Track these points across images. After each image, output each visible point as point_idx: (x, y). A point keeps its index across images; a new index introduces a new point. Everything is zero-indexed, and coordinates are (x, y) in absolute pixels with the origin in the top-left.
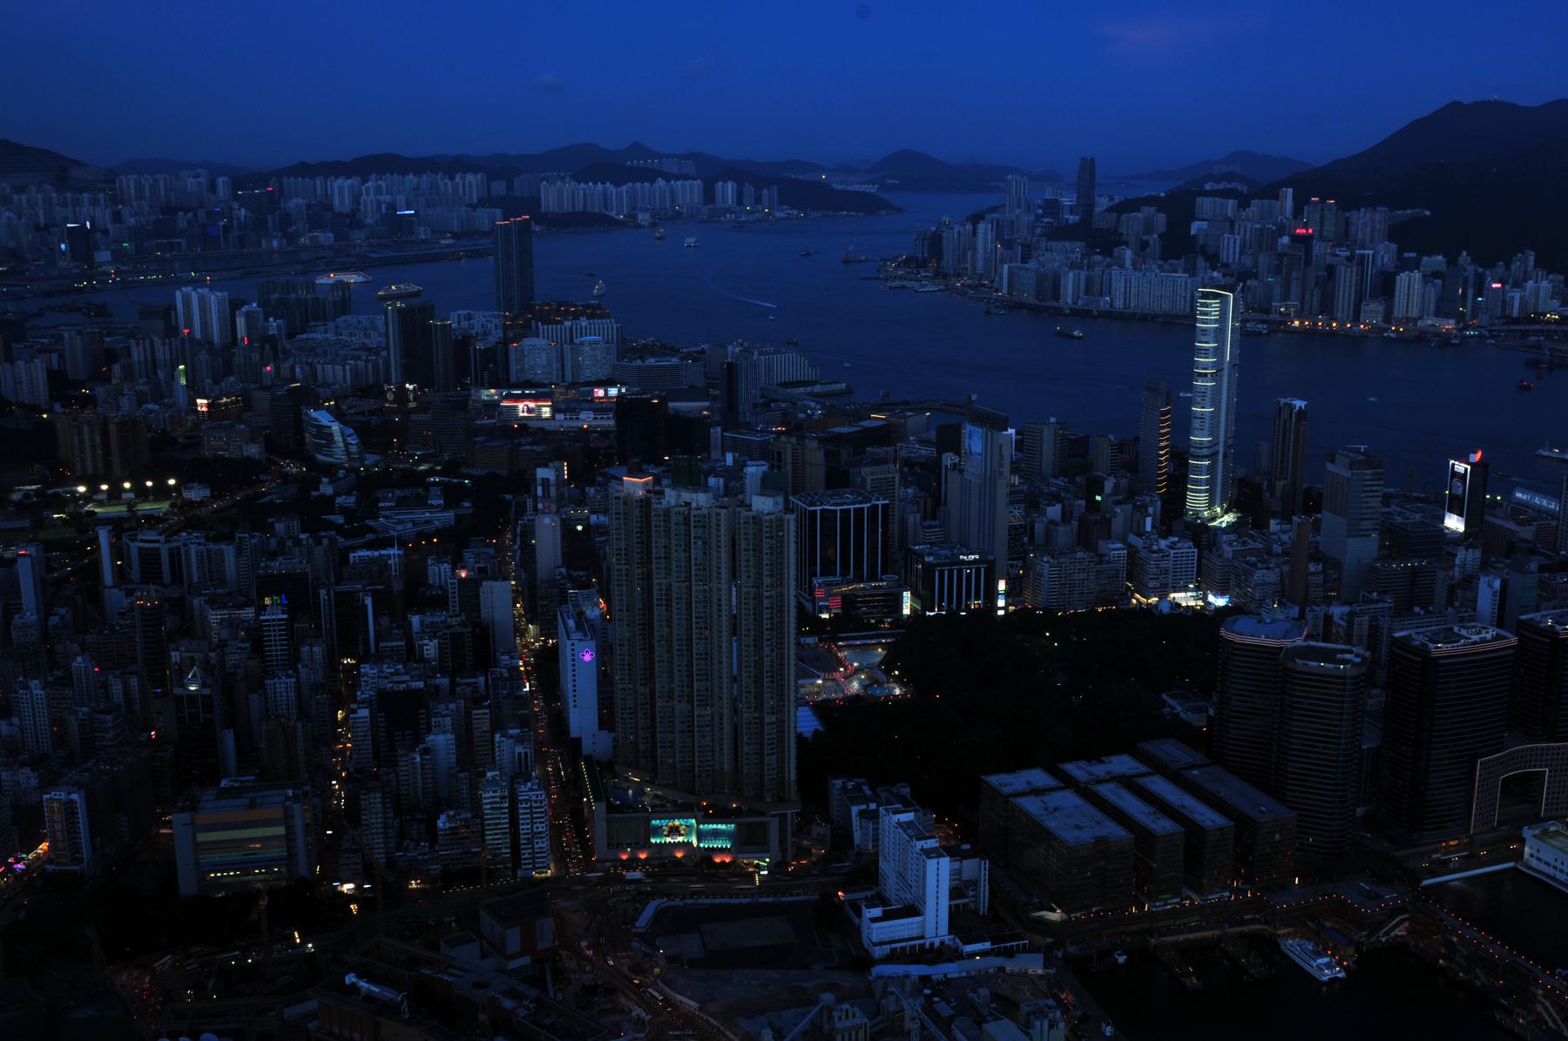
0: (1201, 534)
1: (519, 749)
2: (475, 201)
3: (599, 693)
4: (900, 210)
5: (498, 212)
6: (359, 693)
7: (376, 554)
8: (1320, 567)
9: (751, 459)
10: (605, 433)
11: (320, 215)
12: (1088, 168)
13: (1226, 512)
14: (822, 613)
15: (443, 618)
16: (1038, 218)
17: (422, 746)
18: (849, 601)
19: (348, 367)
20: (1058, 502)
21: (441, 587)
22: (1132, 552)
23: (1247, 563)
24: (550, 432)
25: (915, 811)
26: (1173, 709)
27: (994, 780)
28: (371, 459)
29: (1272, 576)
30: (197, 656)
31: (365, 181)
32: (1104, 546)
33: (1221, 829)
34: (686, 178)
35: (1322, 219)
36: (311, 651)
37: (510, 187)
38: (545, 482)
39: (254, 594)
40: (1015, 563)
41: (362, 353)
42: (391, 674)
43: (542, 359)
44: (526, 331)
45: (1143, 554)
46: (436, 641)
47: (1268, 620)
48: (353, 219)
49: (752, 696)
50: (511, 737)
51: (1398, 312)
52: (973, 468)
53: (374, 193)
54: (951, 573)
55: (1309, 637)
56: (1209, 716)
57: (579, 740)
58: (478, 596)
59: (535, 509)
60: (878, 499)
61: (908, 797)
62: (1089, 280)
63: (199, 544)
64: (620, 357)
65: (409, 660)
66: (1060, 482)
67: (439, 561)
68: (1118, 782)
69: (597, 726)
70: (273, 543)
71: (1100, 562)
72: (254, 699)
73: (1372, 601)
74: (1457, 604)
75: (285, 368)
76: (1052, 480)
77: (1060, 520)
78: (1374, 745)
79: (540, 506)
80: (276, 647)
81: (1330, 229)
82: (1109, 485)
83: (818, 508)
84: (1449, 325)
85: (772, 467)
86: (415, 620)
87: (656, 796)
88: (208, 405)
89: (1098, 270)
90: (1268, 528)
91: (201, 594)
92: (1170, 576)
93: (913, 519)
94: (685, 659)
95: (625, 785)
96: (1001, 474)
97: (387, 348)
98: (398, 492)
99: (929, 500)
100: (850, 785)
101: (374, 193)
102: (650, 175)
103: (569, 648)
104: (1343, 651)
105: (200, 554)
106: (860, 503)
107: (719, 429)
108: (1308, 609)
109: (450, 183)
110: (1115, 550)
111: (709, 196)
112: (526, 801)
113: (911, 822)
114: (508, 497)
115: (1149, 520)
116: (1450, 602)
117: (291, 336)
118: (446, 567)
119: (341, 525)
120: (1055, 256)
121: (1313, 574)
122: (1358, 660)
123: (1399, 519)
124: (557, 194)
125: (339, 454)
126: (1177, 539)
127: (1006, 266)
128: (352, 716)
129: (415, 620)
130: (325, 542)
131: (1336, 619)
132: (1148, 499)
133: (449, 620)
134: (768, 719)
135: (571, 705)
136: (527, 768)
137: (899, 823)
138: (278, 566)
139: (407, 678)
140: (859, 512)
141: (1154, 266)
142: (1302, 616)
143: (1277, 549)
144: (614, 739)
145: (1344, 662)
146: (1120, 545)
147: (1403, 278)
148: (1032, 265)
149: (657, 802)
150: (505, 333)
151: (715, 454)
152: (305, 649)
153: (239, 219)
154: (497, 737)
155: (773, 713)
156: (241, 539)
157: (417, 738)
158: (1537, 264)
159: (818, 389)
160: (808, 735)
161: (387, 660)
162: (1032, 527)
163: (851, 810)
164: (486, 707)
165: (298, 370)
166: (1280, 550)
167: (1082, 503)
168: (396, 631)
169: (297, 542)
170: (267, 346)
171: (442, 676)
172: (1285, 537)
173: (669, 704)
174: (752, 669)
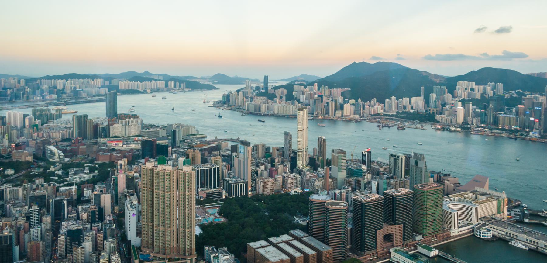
0: (300, 172)
1: (112, 245)
2: (100, 86)
3: (137, 226)
4: (218, 89)
5: (107, 90)
6: (61, 231)
7: (68, 188)
8: (332, 180)
9: (180, 156)
10: (138, 150)
11: (53, 90)
12: (266, 78)
13: (307, 166)
14: (200, 198)
15: (89, 206)
16: (254, 91)
17: (81, 246)
18: (208, 195)
19: (60, 133)
20: (264, 165)
21: (88, 197)
22: (284, 177)
23: (314, 180)
24: (122, 150)
25: (229, 255)
26: (297, 220)
27: (251, 244)
28: (67, 160)
29: (320, 183)
30: (8, 223)
31: (67, 81)
32: (276, 176)
33: (313, 254)
34: (160, 80)
35: (325, 90)
36: (46, 219)
37: (110, 82)
38: (121, 165)
39: (28, 202)
40: (253, 182)
41: (65, 130)
42: (72, 225)
43: (120, 130)
44: (115, 122)
45: (287, 178)
46: (86, 213)
47: (321, 195)
48: (63, 91)
49: (182, 224)
50: (110, 241)
51: (345, 114)
52: (241, 156)
53: (70, 84)
54: (236, 185)
55: (332, 199)
56: (307, 222)
57: (130, 241)
58: (100, 199)
59: (117, 172)
60: (216, 166)
61: (227, 251)
62: (268, 106)
63: (10, 188)
64: (142, 129)
65: (77, 220)
66: (264, 159)
67: (88, 189)
68: (285, 243)
69: (136, 236)
70: (34, 186)
71: (275, 181)
72: (26, 236)
73: (346, 189)
74: (367, 189)
75: (40, 134)
76: (262, 159)
77: (264, 169)
78: (350, 228)
79: (119, 171)
80: (34, 219)
81: (327, 93)
82: (277, 160)
83: (200, 169)
84: (357, 116)
85: (186, 158)
86: (80, 207)
87: (154, 256)
88: (15, 146)
89: (270, 104)
90: (318, 170)
91: (10, 203)
92: (294, 184)
93: (225, 171)
94: (163, 214)
95: (144, 254)
96: (249, 158)
97: (73, 128)
98: (75, 169)
99: (229, 166)
100: (210, 249)
101: (70, 84)
102: (150, 80)
103: (128, 213)
104: (341, 203)
105: (10, 191)
106: (211, 167)
107: (171, 148)
108: (330, 191)
109: (92, 81)
110: (279, 177)
111: (167, 86)
112: (114, 261)
113: (229, 258)
114: (109, 169)
115: (287, 169)
116: (365, 188)
117: (42, 125)
118: (90, 191)
119: (57, 180)
120: (259, 100)
121: (330, 182)
122: (345, 205)
123: (350, 167)
124: (123, 85)
125: (57, 158)
126: (295, 174)
127: (246, 103)
128: (59, 238)
129: (80, 207)
130: (52, 185)
131: (337, 194)
132: (287, 163)
133: (91, 207)
134: (187, 230)
135: (128, 230)
136: (114, 251)
137: (225, 259)
138: (36, 193)
139: (77, 225)
140: (211, 170)
141: (284, 103)
142: (328, 194)
143: (321, 175)
144: (141, 240)
145: (341, 206)
146: (280, 176)
147: (345, 105)
148: (253, 103)
149: (154, 258)
150: (109, 122)
151: (170, 155)
152: (44, 219)
153: (27, 91)
154: (105, 242)
155: (188, 229)
156: (24, 185)
157: (80, 244)
158: (377, 101)
159: (198, 136)
160: (198, 234)
161: (70, 220)
162: (257, 172)
163: (210, 256)
164: (102, 233)
165: (44, 134)
166: (321, 176)
167: (270, 165)
168: (73, 211)
169: (43, 186)
170: (35, 128)
171: (88, 224)
172: (322, 172)
173: (158, 228)
174: (183, 216)
